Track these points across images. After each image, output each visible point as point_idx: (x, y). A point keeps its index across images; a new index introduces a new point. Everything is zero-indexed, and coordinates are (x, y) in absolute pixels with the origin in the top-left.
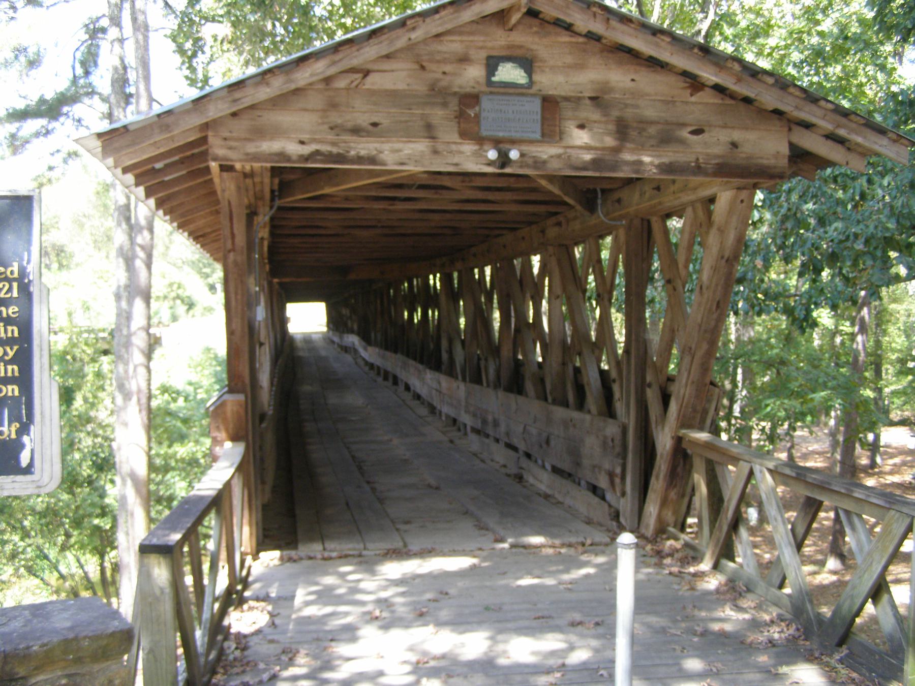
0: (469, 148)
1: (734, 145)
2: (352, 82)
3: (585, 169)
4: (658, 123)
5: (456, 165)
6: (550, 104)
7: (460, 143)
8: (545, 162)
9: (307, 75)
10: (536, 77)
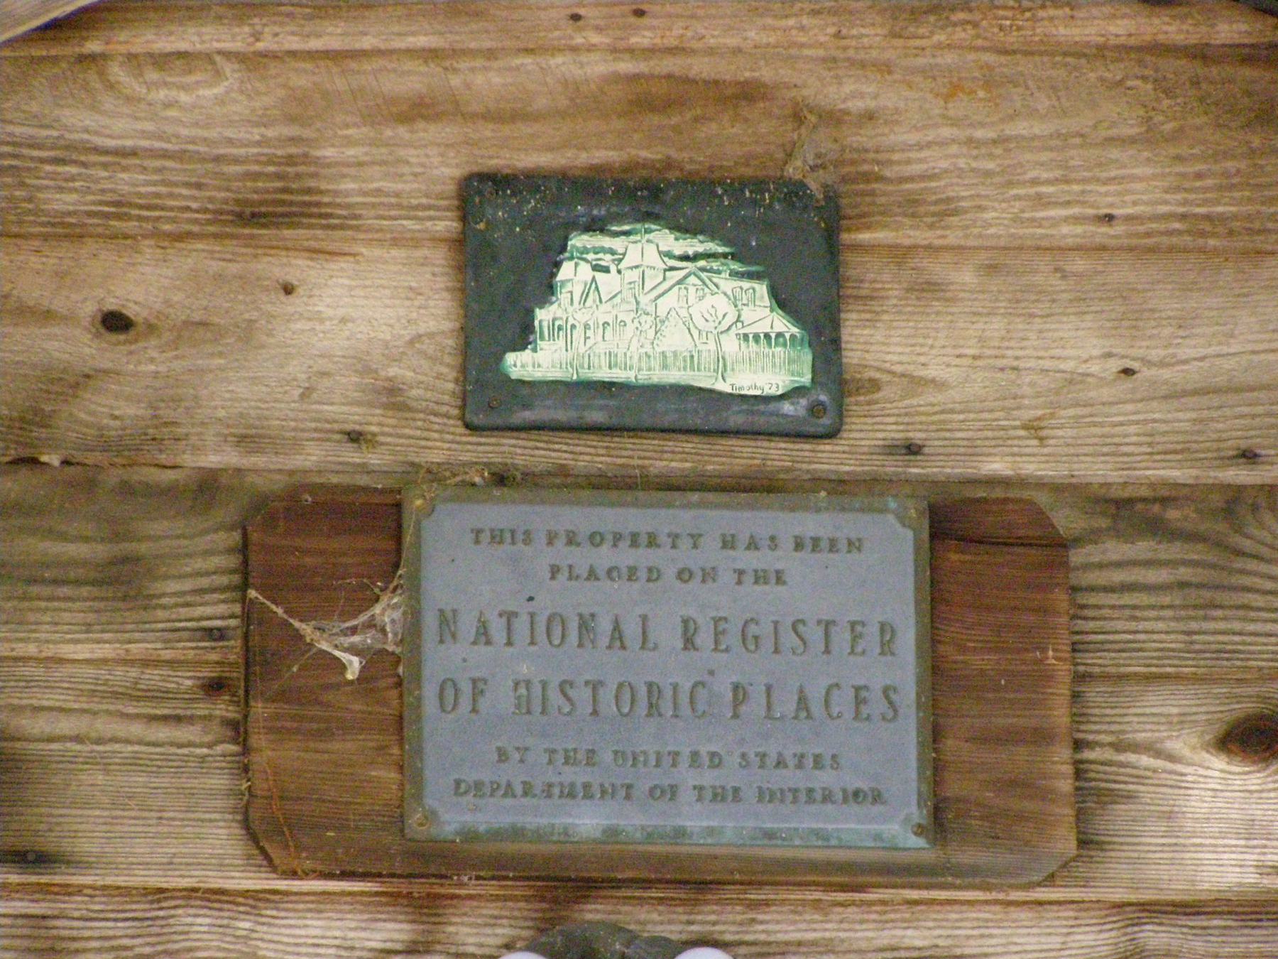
7: (256, 899)
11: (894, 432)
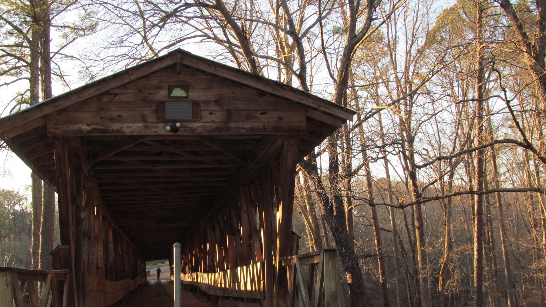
0: (161, 125)
1: (280, 118)
2: (110, 99)
3: (213, 131)
4: (246, 110)
5: (156, 132)
6: (196, 104)
8: (195, 129)
9: (87, 95)
10: (190, 94)
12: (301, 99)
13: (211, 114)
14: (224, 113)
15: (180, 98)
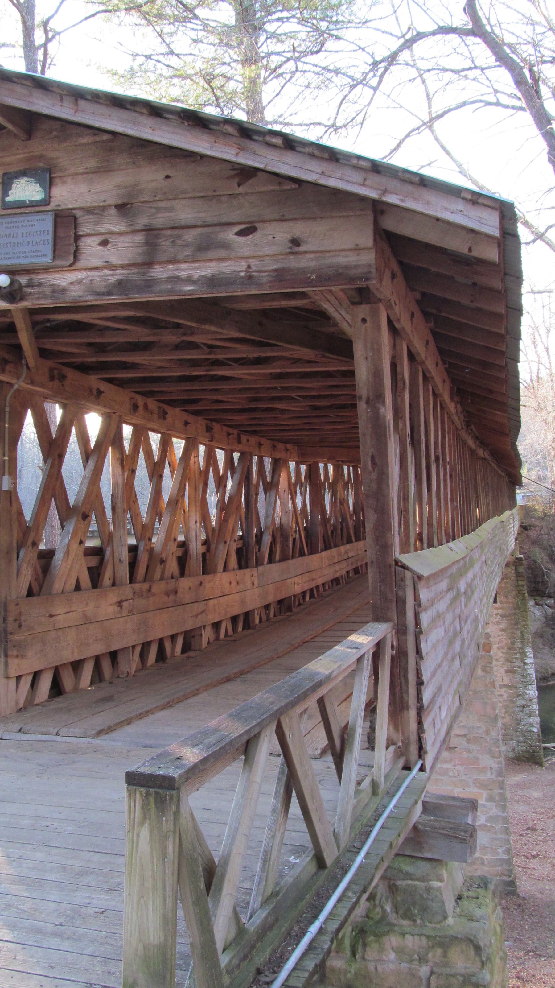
1: (296, 242)
3: (109, 294)
4: (195, 226)
8: (64, 290)
11: (57, 204)
12: (323, 173)
13: (104, 243)
14: (139, 238)
15: (28, 206)
